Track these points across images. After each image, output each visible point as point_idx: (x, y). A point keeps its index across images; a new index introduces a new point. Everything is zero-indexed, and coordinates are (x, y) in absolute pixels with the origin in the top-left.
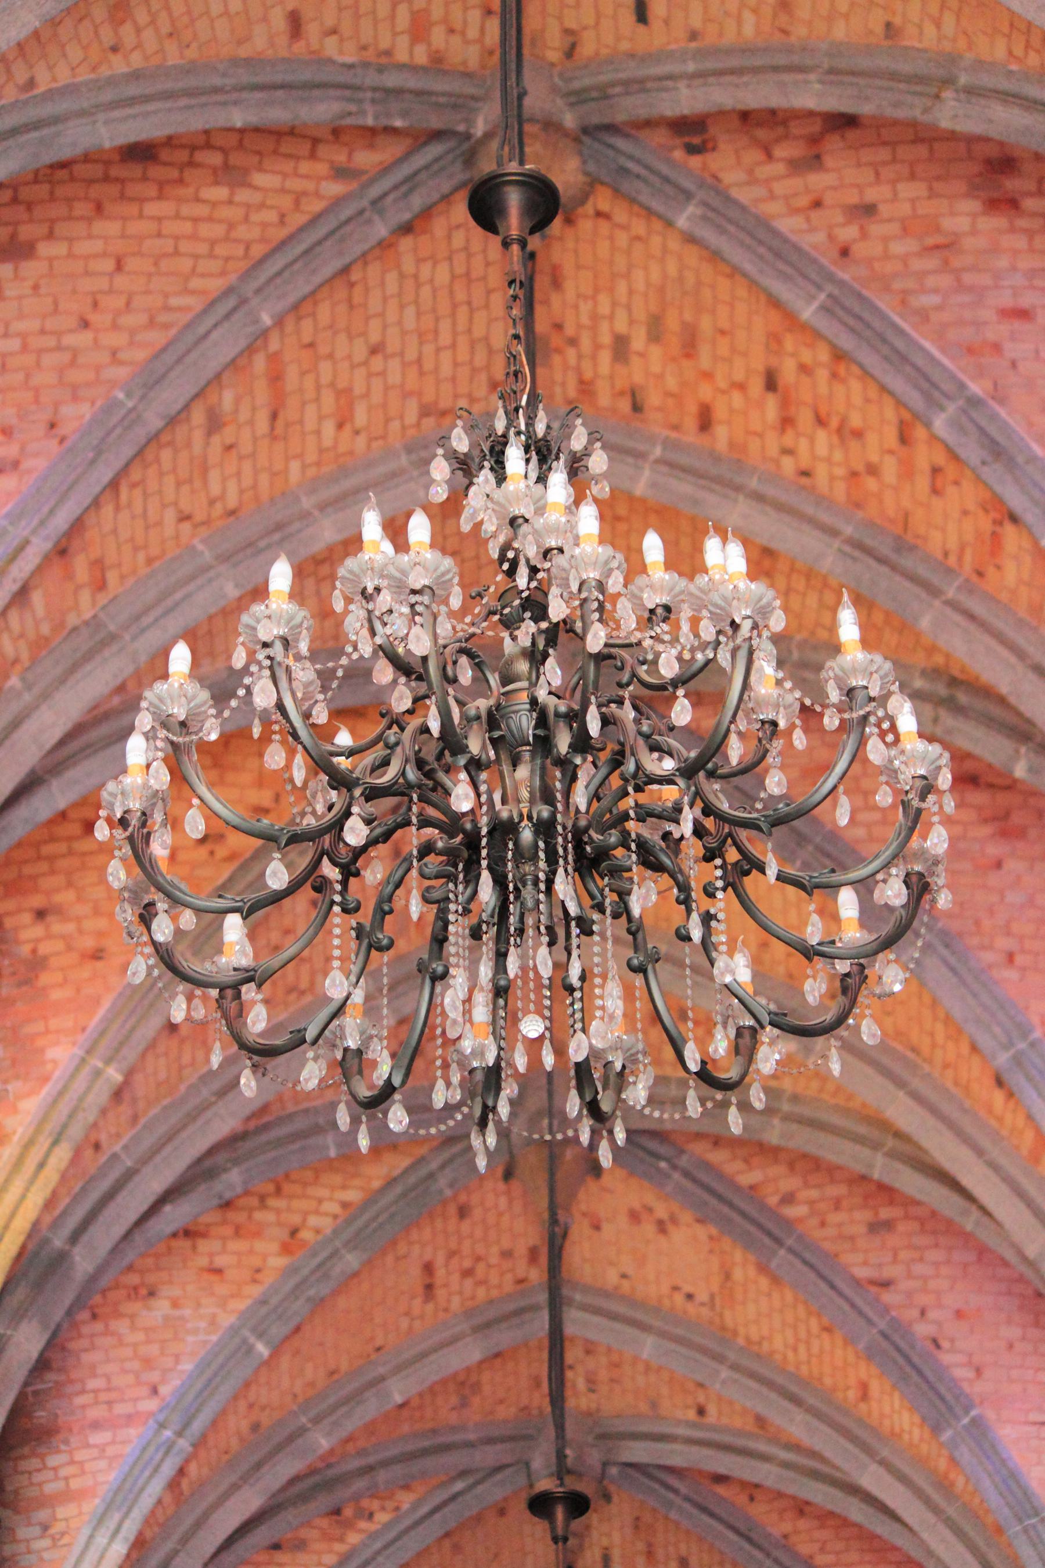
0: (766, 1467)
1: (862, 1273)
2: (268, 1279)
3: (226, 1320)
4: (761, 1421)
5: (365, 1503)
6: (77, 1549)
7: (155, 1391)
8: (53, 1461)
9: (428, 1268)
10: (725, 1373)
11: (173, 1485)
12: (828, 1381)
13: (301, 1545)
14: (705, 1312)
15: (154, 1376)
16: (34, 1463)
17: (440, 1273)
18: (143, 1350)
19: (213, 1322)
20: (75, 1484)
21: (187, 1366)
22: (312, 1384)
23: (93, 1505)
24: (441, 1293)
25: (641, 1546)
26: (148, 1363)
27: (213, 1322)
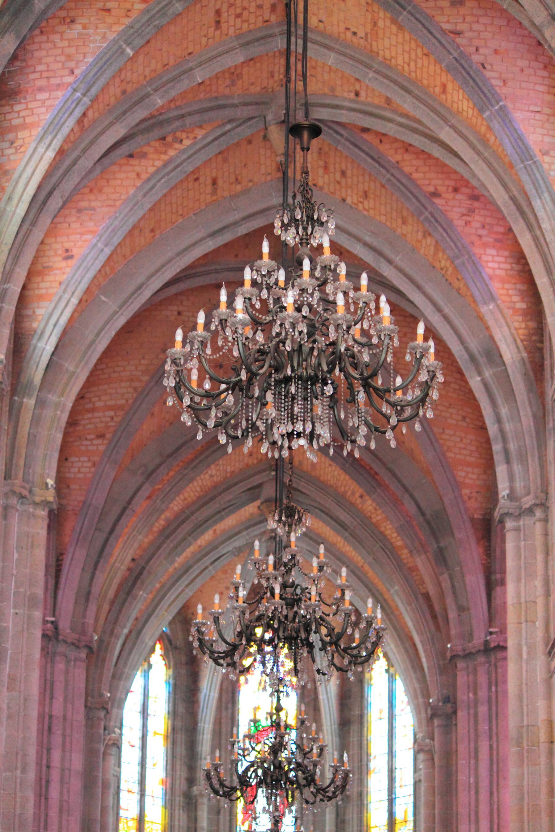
0: (390, 125)
1: (446, 26)
2: (134, 15)
3: (111, 36)
4: (388, 101)
5: (178, 134)
6: (28, 154)
7: (72, 72)
8: (17, 108)
9: (218, 13)
10: (371, 75)
11: (80, 121)
12: (425, 82)
13: (144, 155)
14: (362, 42)
15: (72, 64)
16: (7, 109)
17: (224, 15)
18: (67, 50)
19: (104, 37)
20: (28, 120)
21: (90, 59)
22: (155, 71)
23: (37, 131)
24: (224, 26)
25: (321, 163)
26: (69, 57)
27: (104, 37)
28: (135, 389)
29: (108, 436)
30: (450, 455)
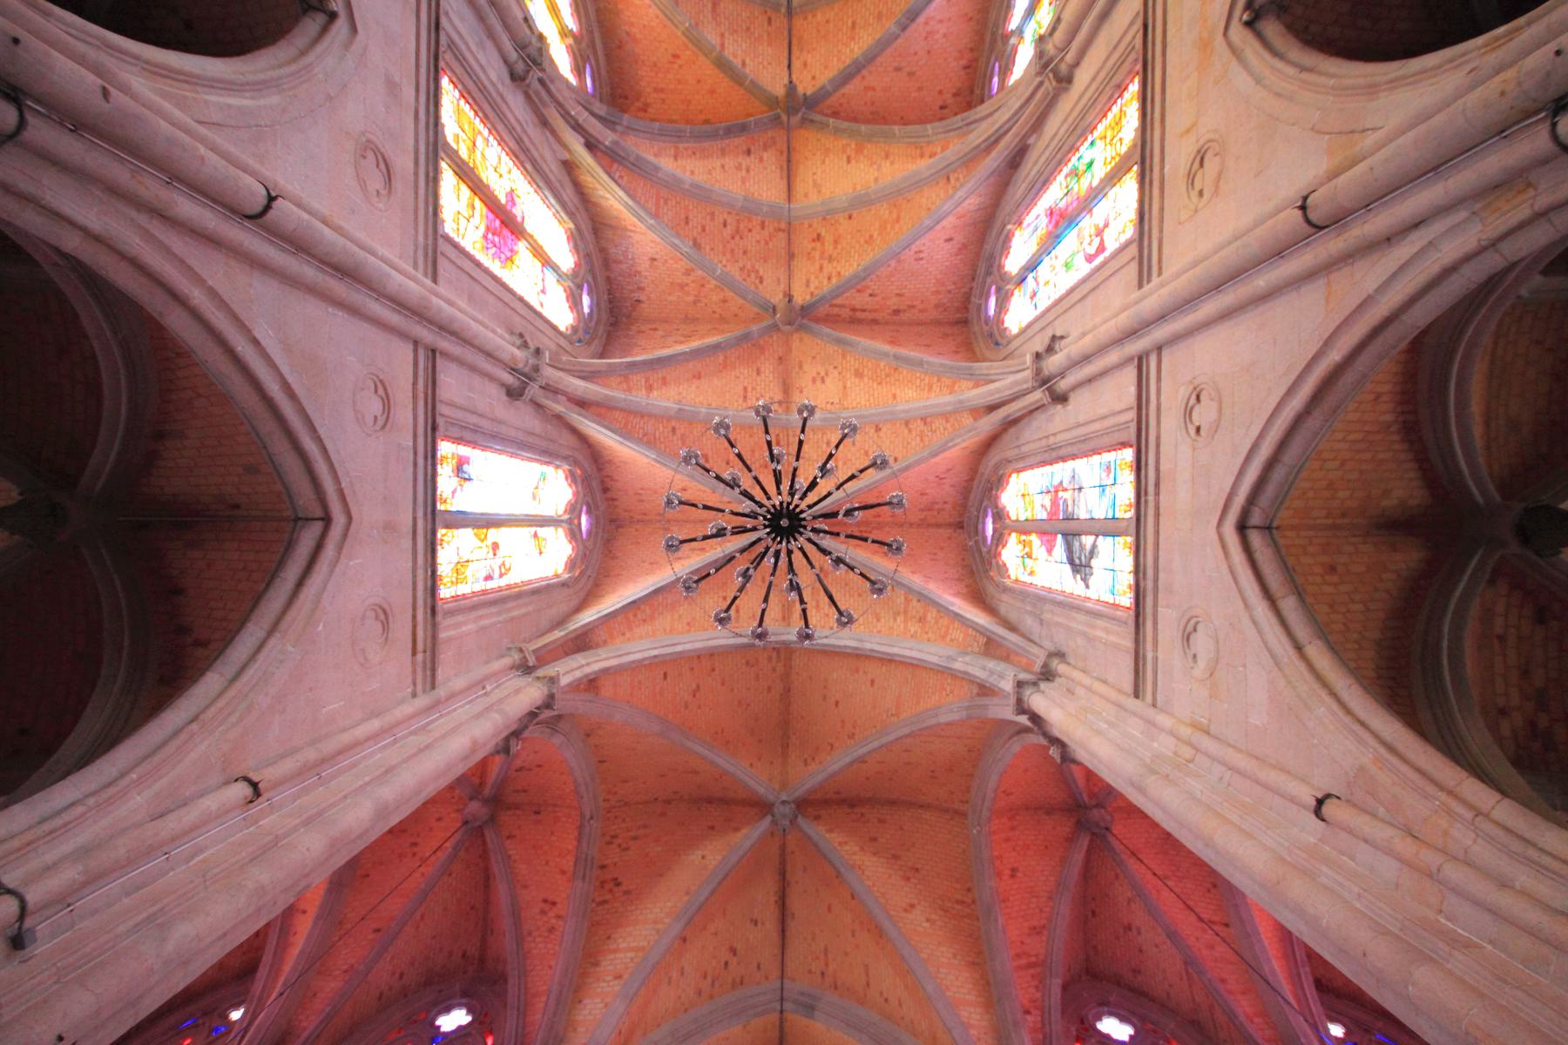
28: (658, 931)
29: (625, 977)
30: (949, 994)
